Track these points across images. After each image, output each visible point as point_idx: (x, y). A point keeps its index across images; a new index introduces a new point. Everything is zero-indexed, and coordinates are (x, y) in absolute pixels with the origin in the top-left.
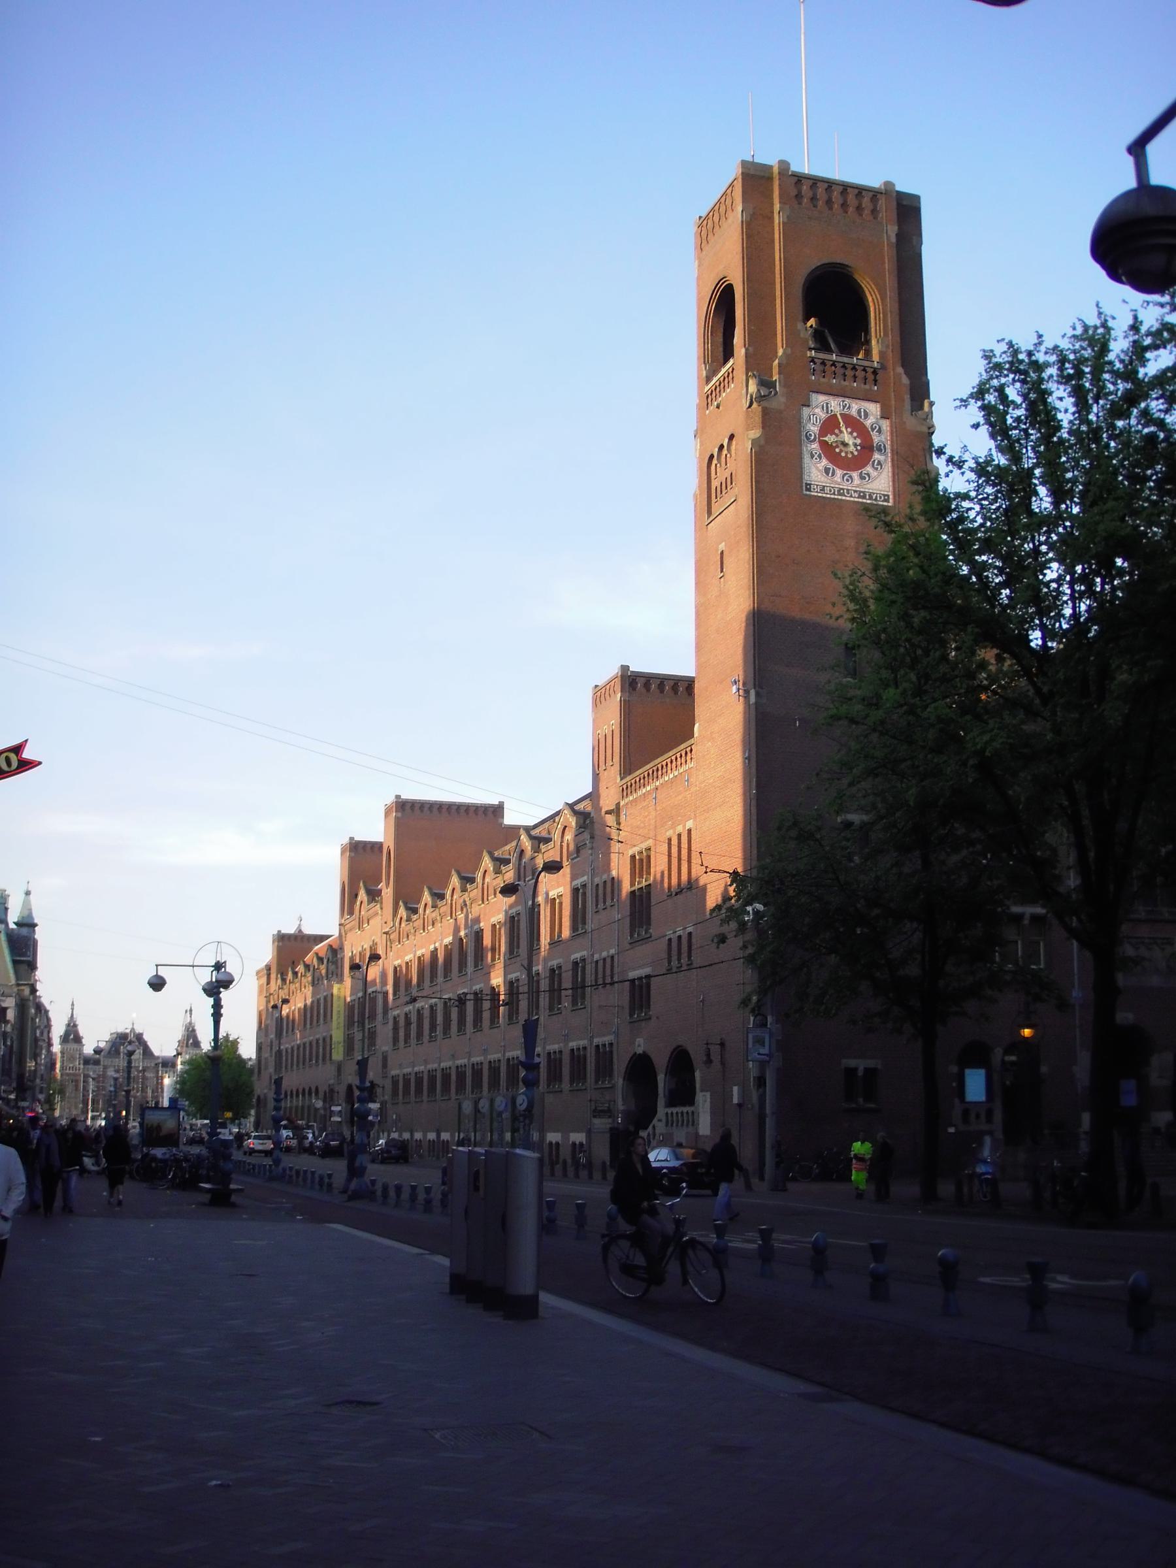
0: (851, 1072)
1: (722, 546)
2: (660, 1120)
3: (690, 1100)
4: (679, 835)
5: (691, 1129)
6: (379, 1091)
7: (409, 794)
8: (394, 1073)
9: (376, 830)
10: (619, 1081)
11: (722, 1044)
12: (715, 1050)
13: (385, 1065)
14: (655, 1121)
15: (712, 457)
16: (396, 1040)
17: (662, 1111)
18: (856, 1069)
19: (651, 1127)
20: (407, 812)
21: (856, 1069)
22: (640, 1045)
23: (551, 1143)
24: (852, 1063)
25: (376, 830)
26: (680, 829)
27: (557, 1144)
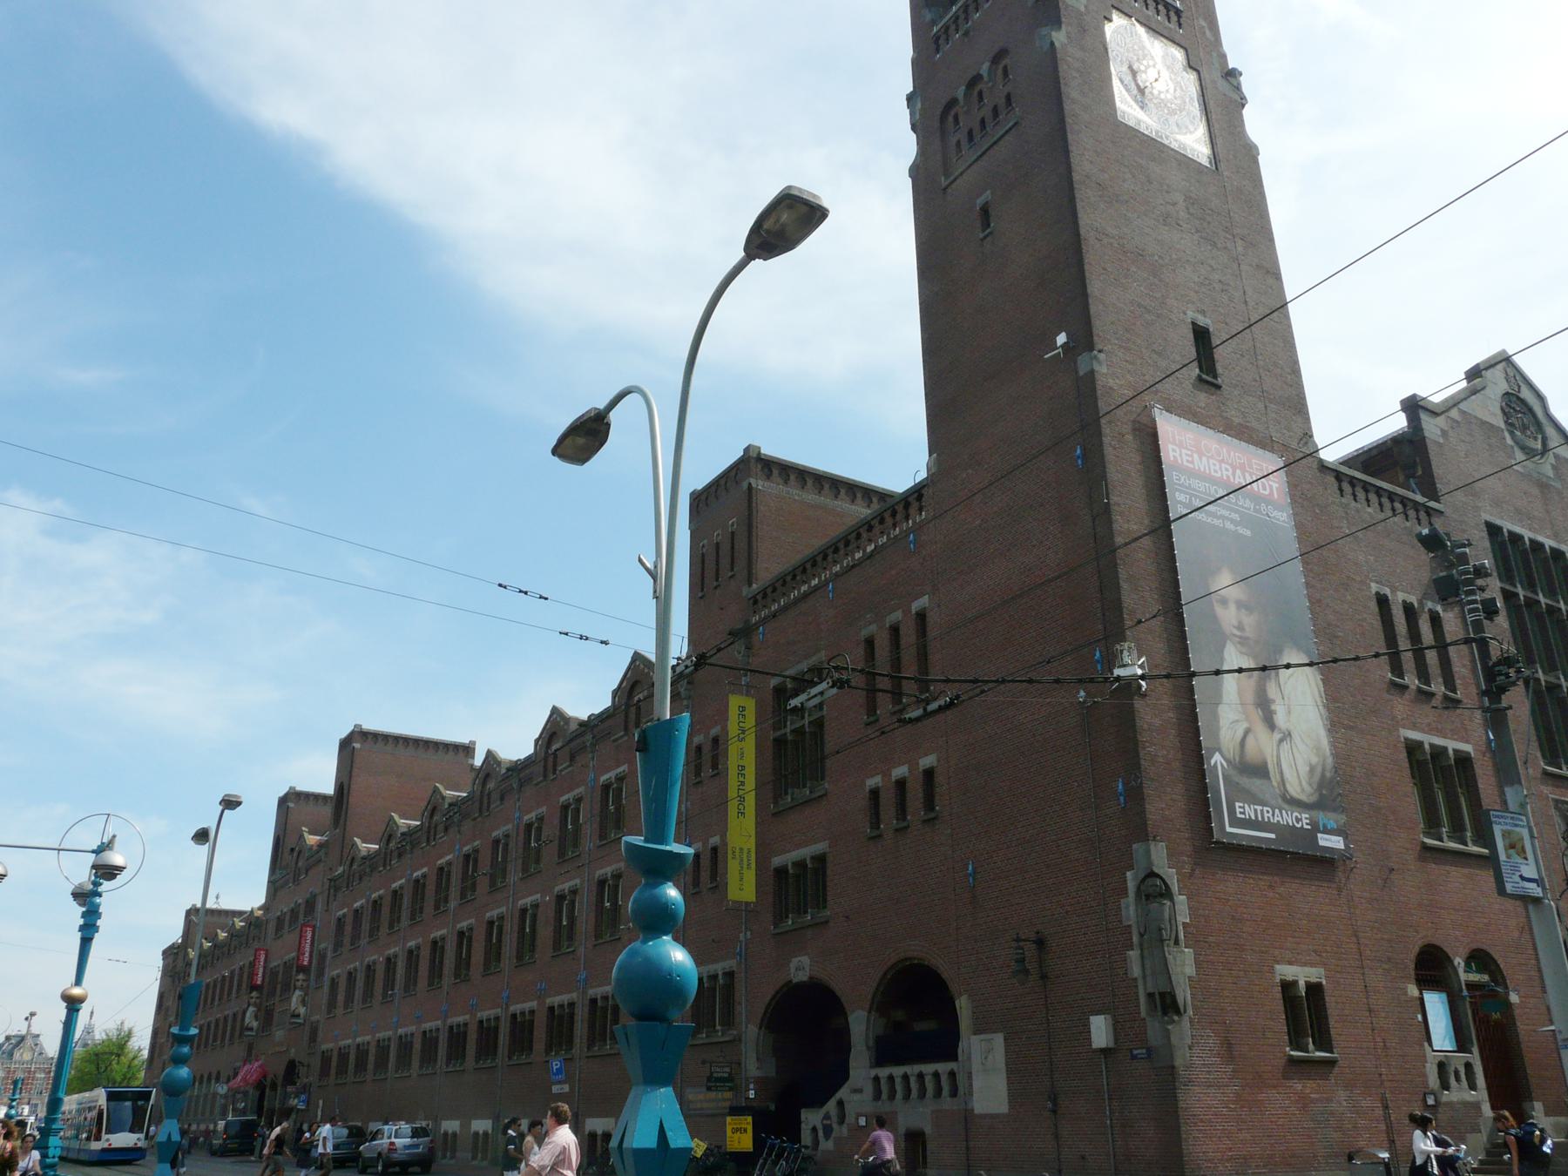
0: (1288, 987)
1: (980, 201)
2: (859, 1091)
3: (945, 1045)
4: (895, 630)
5: (947, 1103)
6: (302, 1071)
7: (370, 725)
8: (324, 1047)
9: (321, 777)
10: (750, 1031)
11: (1040, 943)
12: (1030, 950)
13: (313, 1038)
14: (843, 1093)
15: (953, 102)
16: (332, 1005)
17: (861, 1069)
18: (1295, 983)
19: (831, 1105)
20: (358, 748)
21: (1295, 983)
22: (801, 968)
23: (446, 1134)
24: (1288, 971)
25: (321, 777)
26: (897, 616)
27: (455, 1134)
